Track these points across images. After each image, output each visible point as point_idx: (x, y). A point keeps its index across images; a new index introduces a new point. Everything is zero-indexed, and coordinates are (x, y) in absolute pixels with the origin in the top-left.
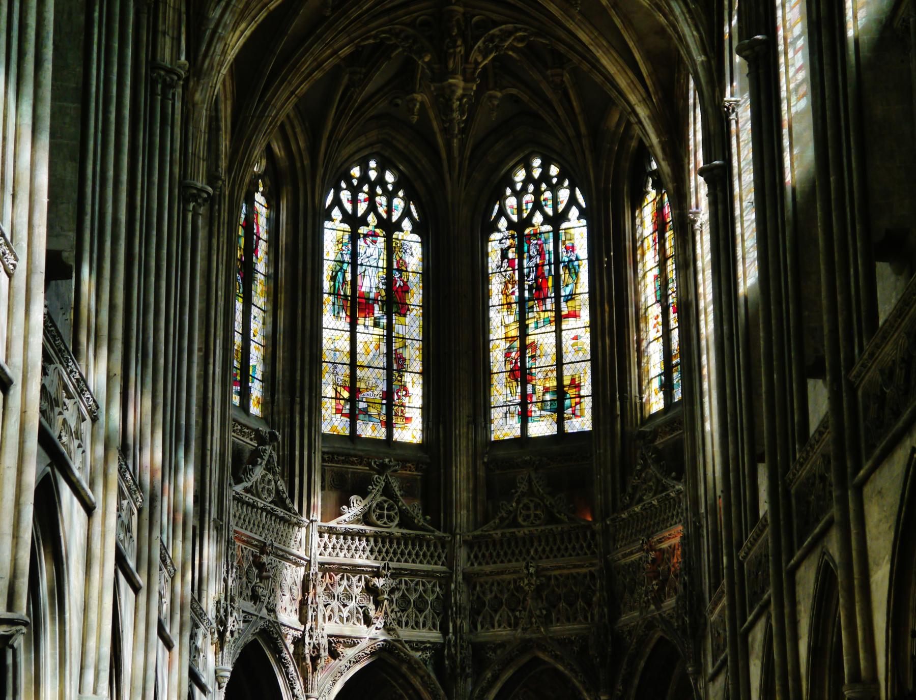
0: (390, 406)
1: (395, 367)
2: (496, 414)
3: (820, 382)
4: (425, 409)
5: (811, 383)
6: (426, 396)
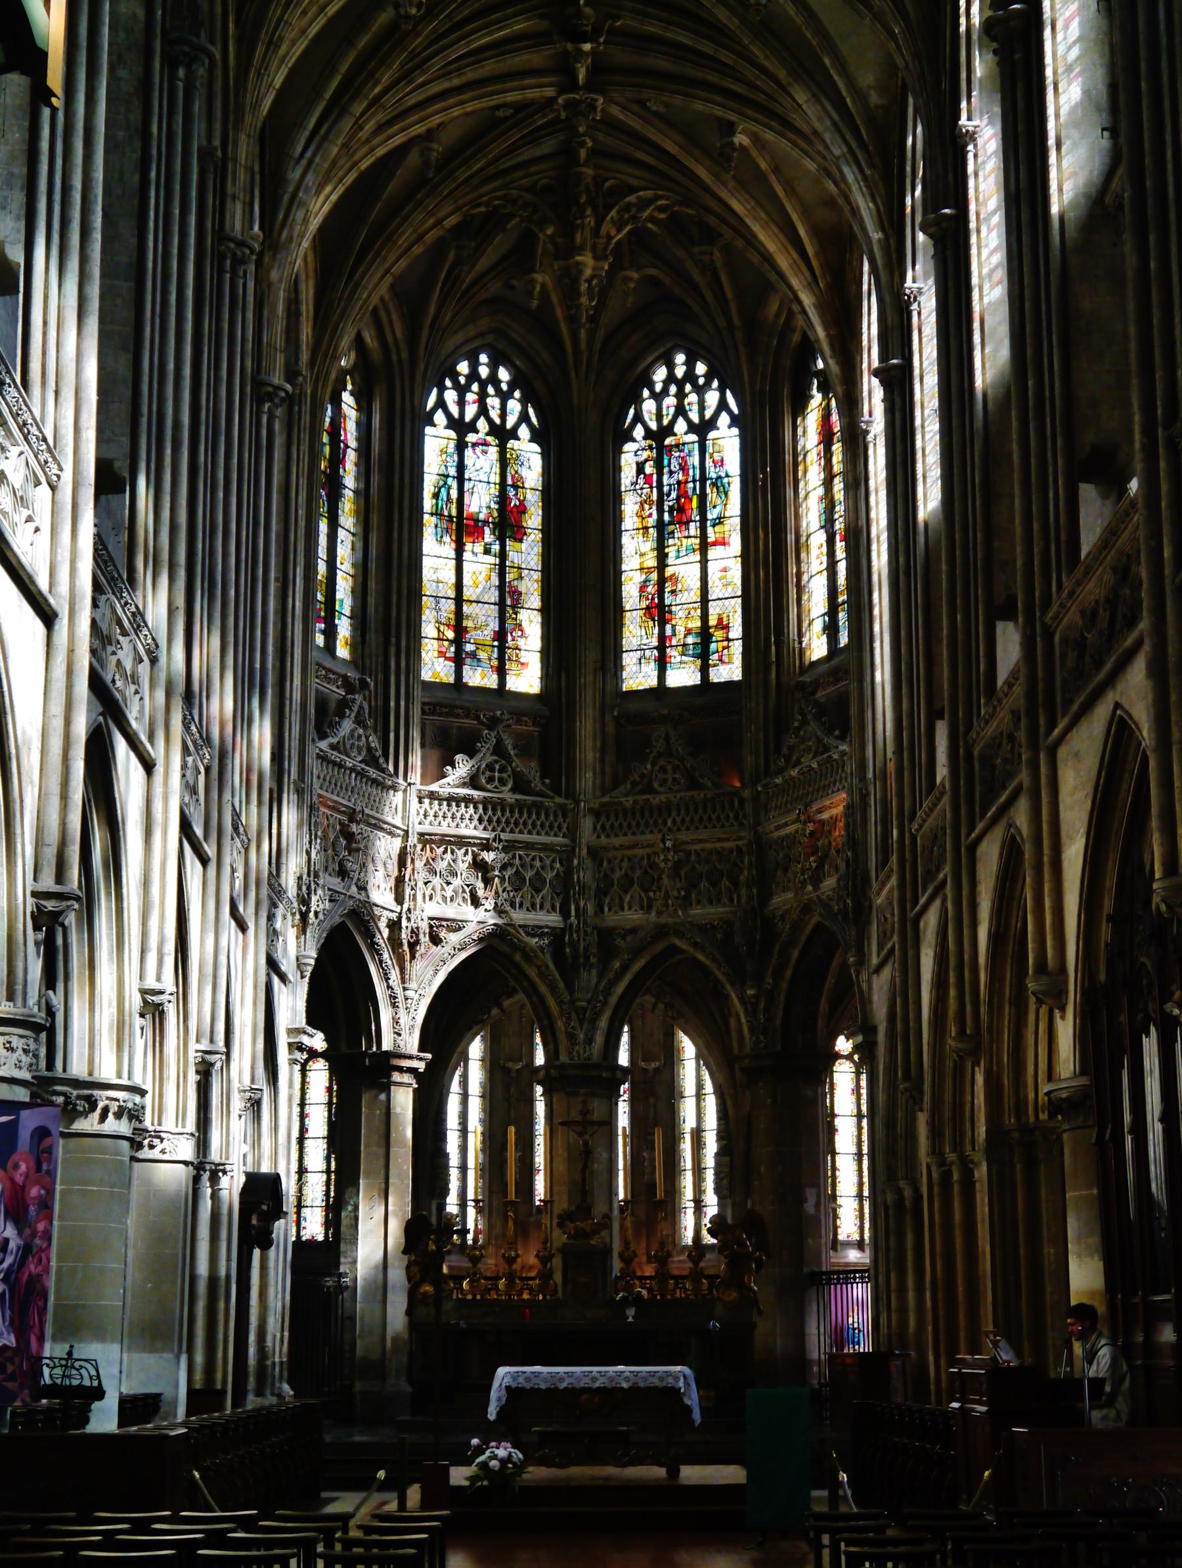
0: (502, 649)
1: (509, 602)
2: (629, 660)
3: (1010, 626)
4: (545, 653)
5: (1000, 626)
6: (546, 637)
